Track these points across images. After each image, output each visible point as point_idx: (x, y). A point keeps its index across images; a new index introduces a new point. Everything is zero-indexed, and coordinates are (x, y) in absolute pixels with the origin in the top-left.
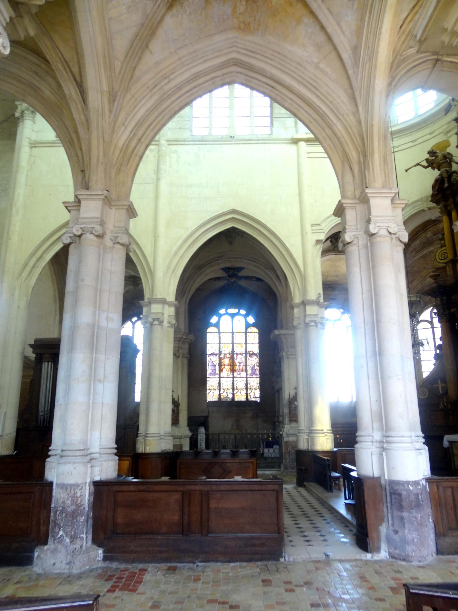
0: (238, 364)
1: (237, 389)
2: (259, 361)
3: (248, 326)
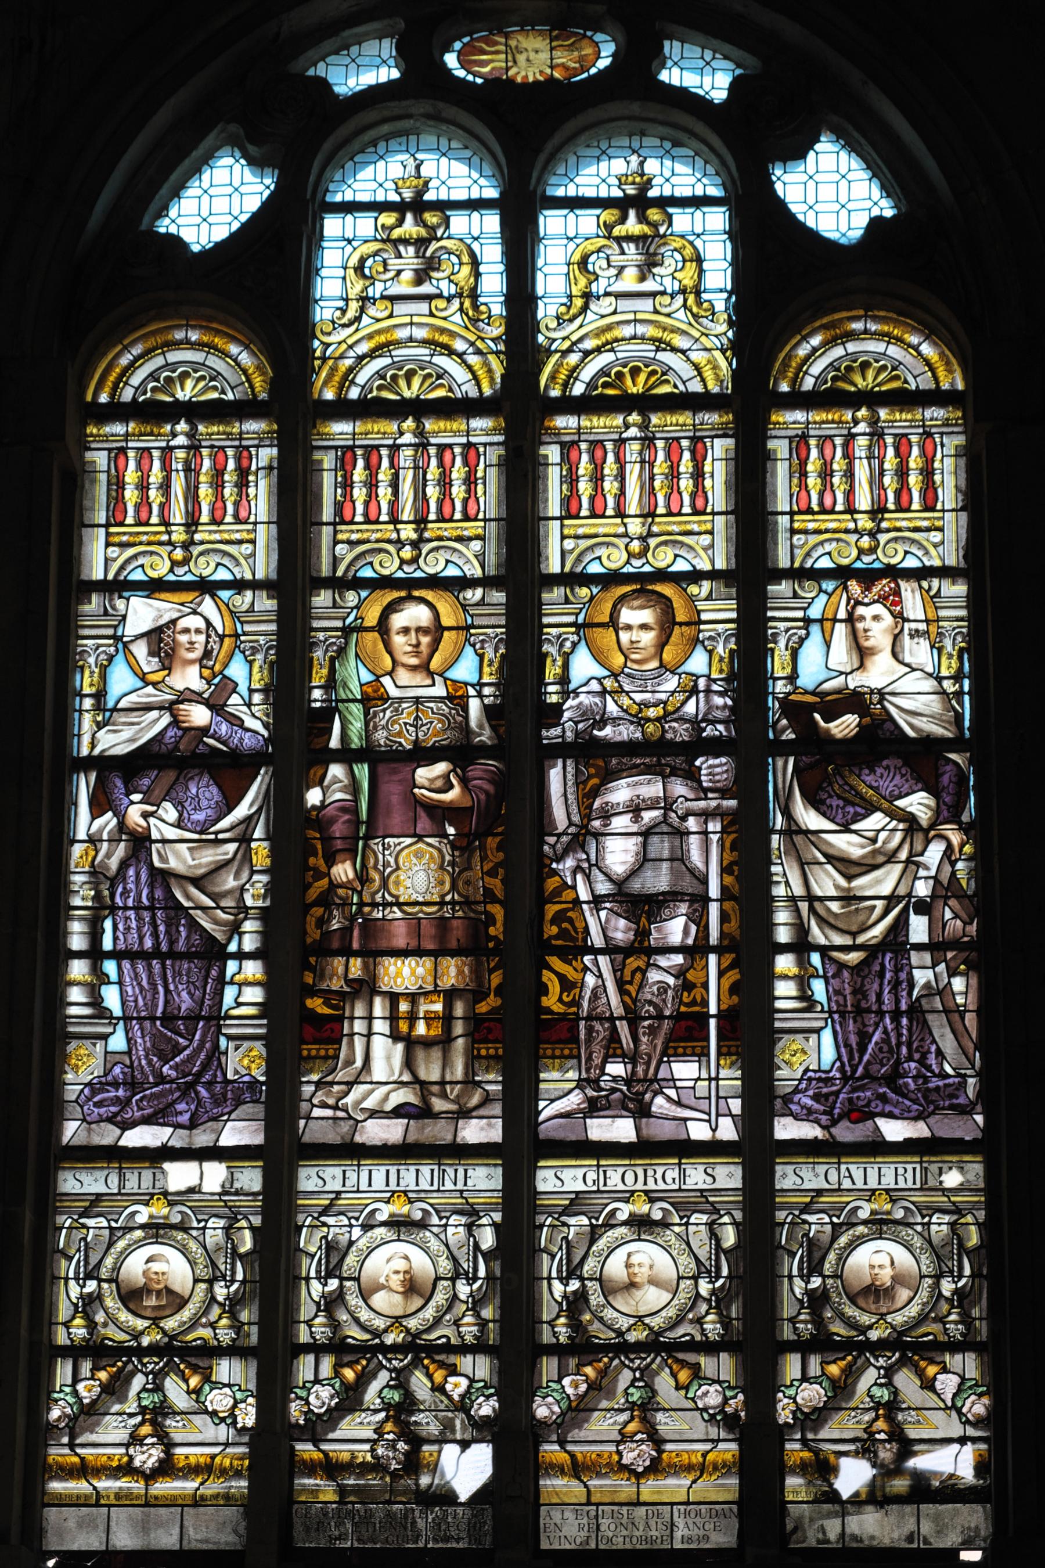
1: (581, 1348)
2: (981, 860)
3: (784, 278)
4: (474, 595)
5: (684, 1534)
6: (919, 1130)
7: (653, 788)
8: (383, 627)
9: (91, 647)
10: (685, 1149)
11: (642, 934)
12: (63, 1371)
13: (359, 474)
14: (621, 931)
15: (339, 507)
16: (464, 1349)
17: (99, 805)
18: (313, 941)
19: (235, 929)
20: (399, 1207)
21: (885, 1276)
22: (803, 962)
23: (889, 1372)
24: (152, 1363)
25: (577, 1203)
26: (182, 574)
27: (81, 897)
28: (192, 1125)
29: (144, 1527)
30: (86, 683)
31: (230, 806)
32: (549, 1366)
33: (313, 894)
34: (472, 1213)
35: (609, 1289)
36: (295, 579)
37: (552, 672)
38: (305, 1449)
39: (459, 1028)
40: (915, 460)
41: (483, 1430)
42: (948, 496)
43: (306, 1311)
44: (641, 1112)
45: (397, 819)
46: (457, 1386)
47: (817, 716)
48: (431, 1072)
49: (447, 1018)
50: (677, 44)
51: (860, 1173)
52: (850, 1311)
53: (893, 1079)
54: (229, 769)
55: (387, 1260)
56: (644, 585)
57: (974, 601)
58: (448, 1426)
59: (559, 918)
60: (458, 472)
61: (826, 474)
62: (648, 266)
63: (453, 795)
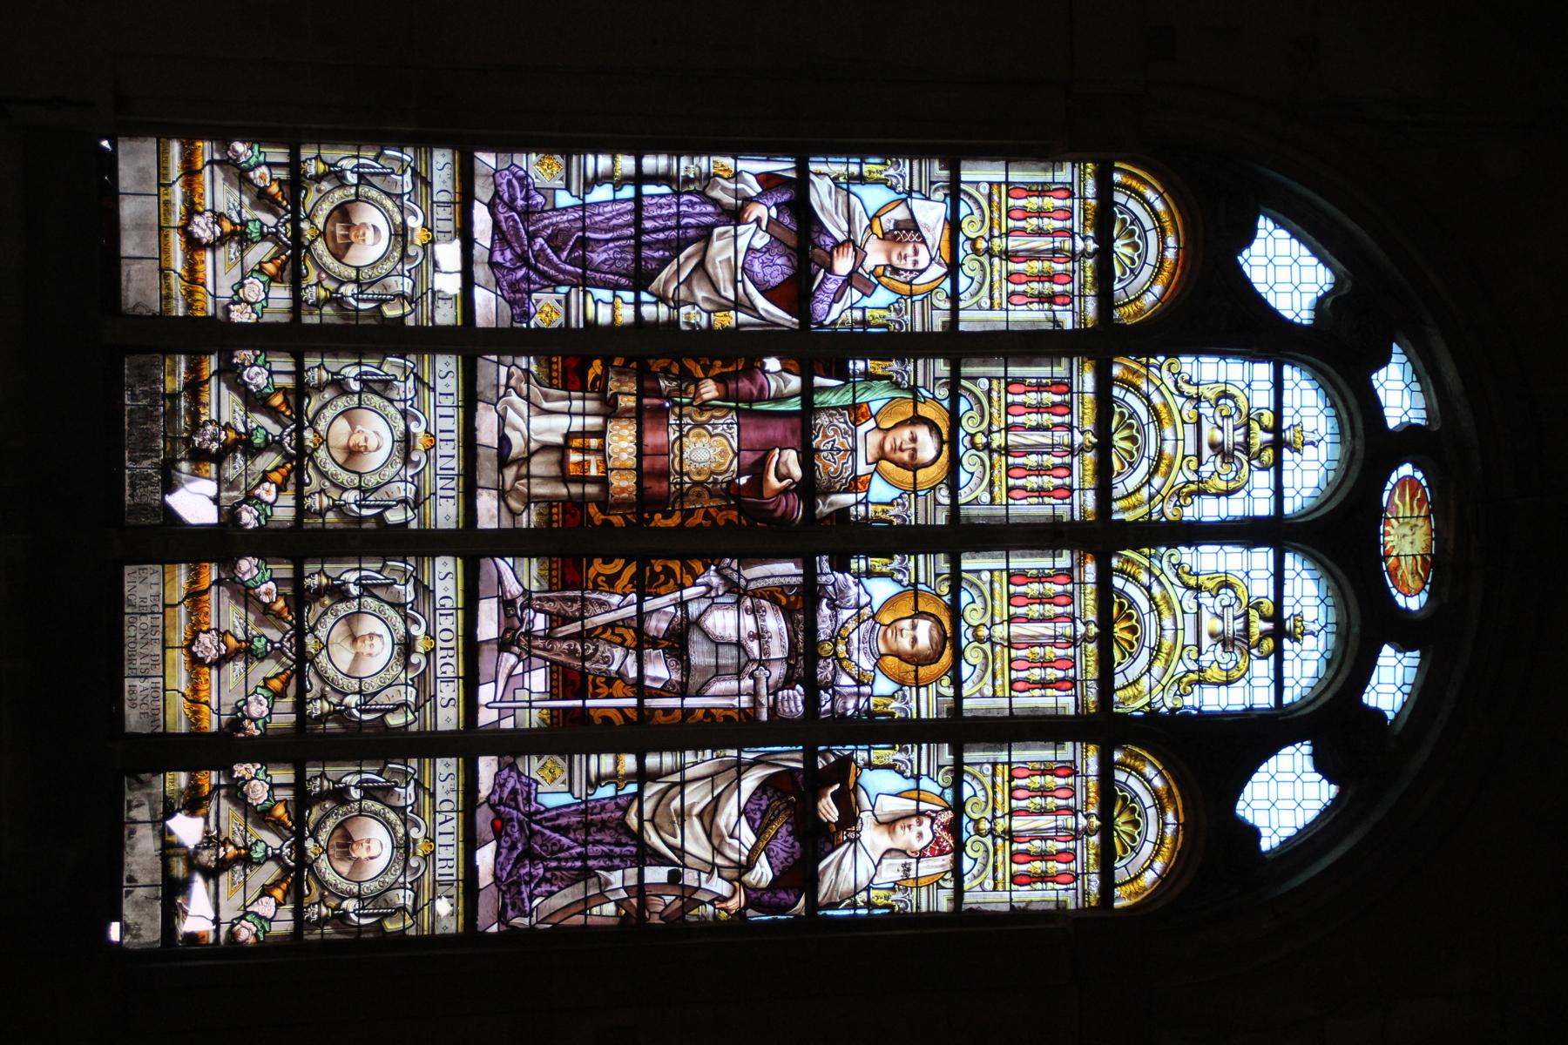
0: (661, 611)
1: (300, 597)
3: (1212, 755)
4: (944, 497)
5: (136, 687)
6: (485, 877)
7: (777, 649)
8: (917, 420)
9: (902, 170)
10: (471, 682)
11: (654, 643)
12: (279, 155)
13: (1049, 397)
14: (657, 626)
15: (1020, 381)
16: (299, 498)
17: (769, 182)
18: (653, 364)
19: (661, 298)
20: (420, 442)
21: (360, 852)
22: (629, 778)
23: (277, 858)
24: (286, 232)
25: (425, 591)
26: (964, 248)
27: (688, 166)
28: (492, 264)
29: (140, 226)
30: (873, 167)
31: (768, 293)
32: (285, 570)
33: (690, 364)
34: (417, 503)
35: (350, 619)
36: (957, 345)
37: (877, 563)
38: (212, 363)
39: (575, 489)
40: (1054, 867)
41: (230, 516)
42: (1024, 895)
43: (332, 364)
44: (503, 645)
45: (753, 435)
46: (267, 492)
47: (837, 787)
48: (539, 466)
49: (583, 479)
50: (1416, 662)
51: (449, 829)
52: (331, 824)
53: (529, 855)
54: (796, 292)
55: (376, 432)
56: (950, 640)
57: (934, 918)
58: (233, 485)
59: (669, 573)
60: (1048, 481)
61: (1043, 792)
62: (1225, 641)
63: (774, 482)
